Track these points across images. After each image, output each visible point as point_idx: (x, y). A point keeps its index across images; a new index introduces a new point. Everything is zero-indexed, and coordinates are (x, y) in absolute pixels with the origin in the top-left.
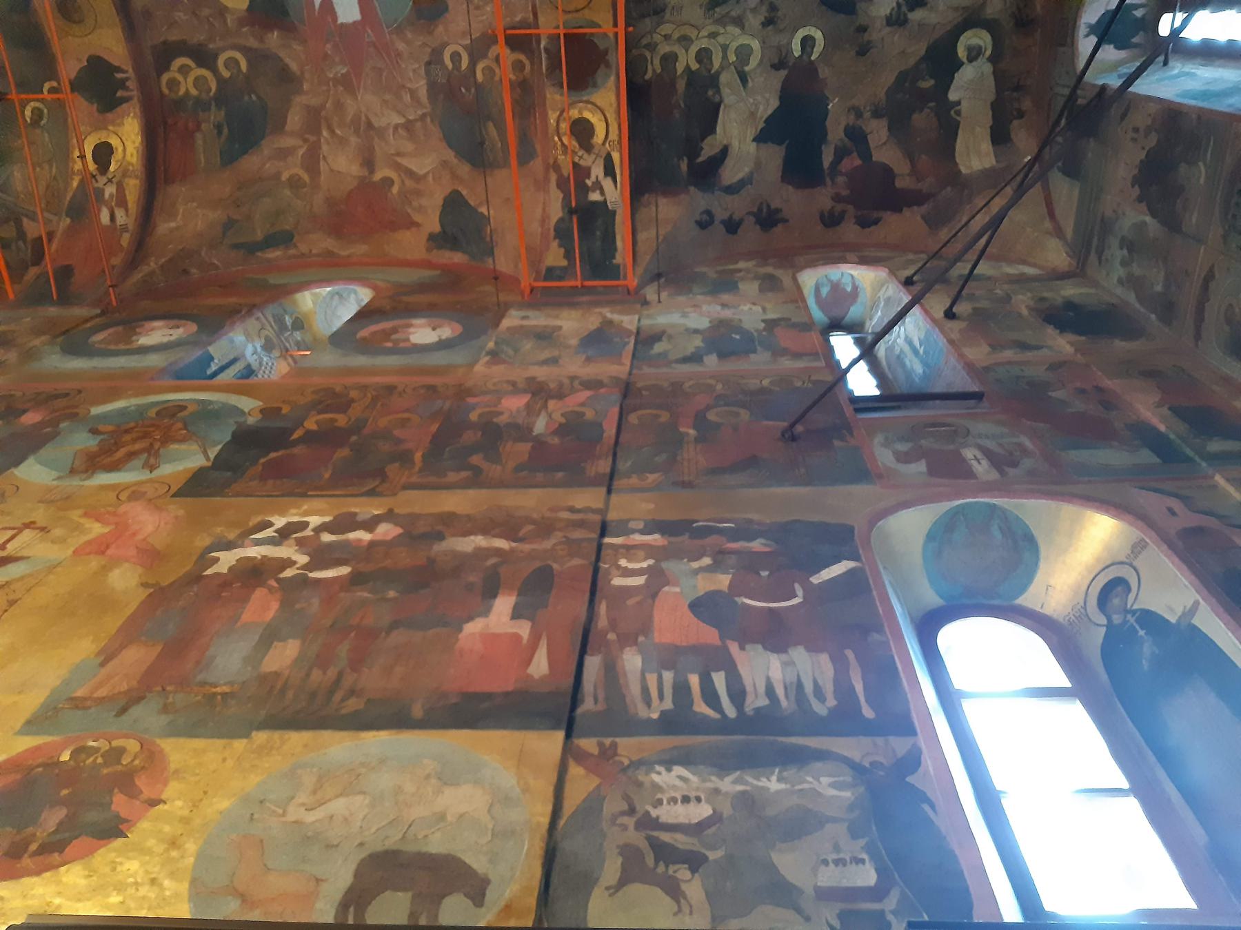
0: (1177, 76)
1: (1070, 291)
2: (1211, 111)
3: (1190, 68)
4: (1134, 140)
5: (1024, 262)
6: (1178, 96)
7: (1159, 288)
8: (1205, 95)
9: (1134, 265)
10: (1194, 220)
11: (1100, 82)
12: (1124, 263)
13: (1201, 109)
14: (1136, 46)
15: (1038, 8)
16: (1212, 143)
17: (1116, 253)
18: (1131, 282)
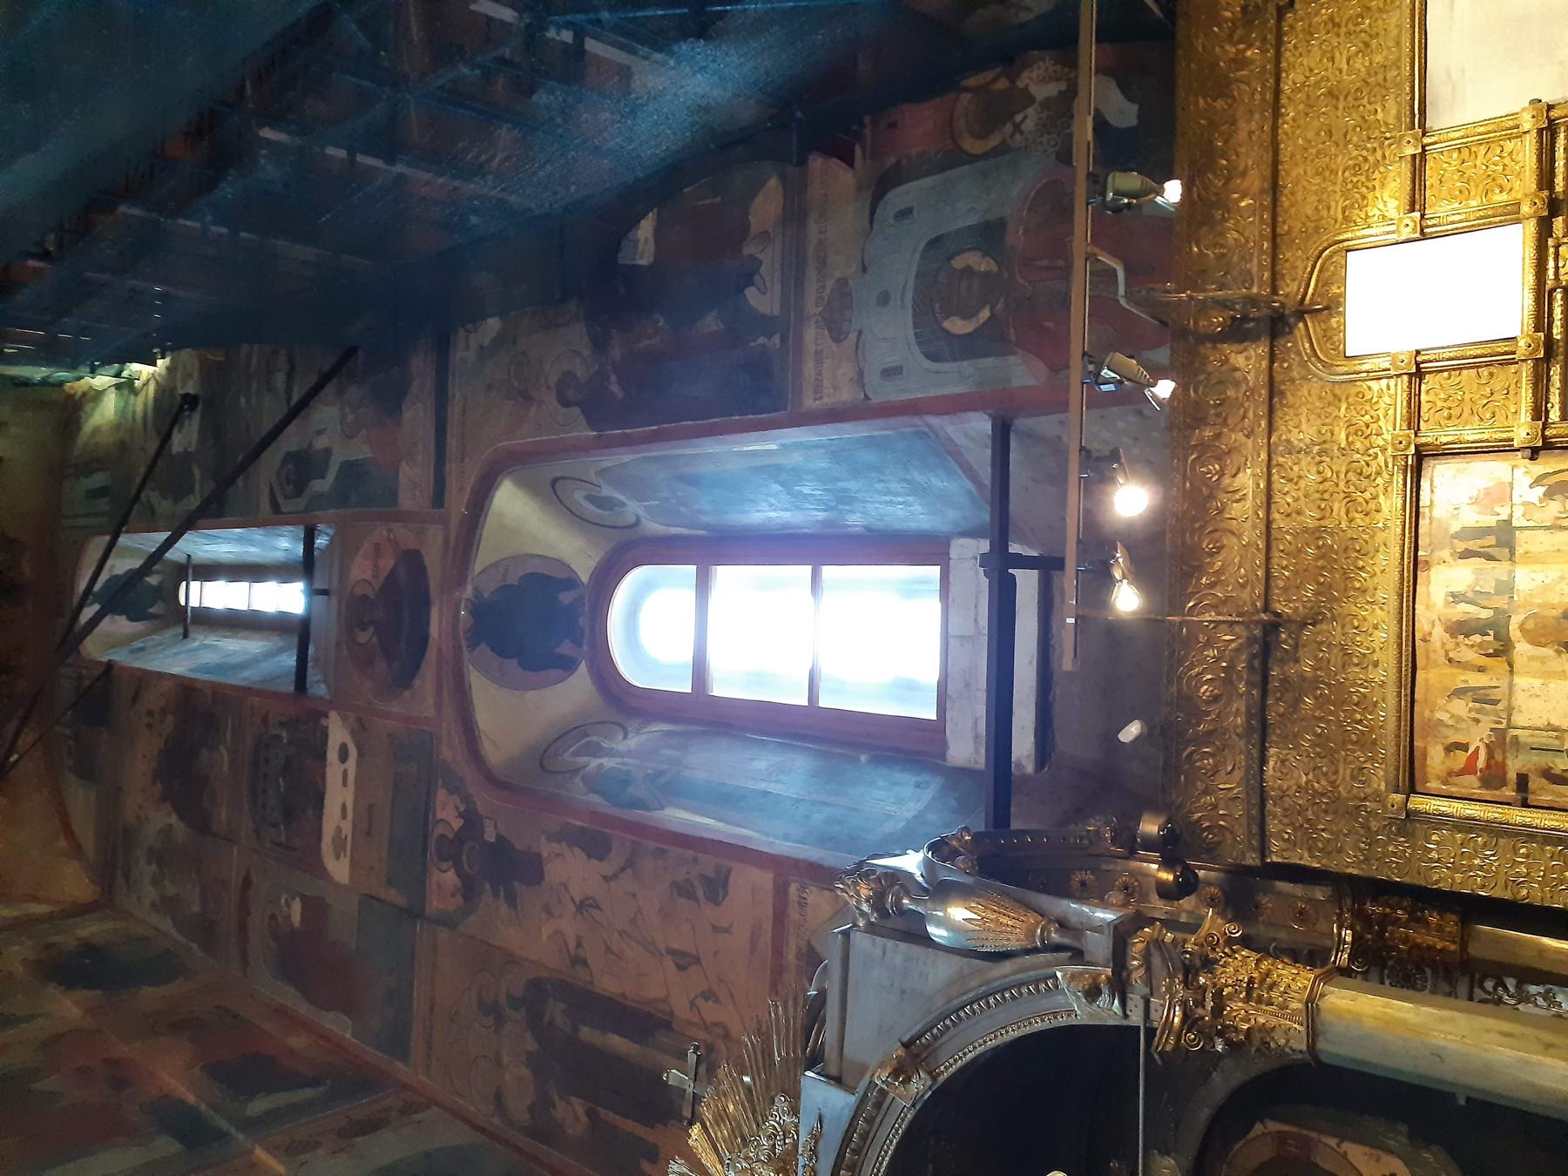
0: (197, 649)
1: (90, 929)
2: (226, 686)
3: (211, 640)
4: (149, 726)
5: (35, 899)
6: (192, 670)
7: (196, 908)
8: (221, 668)
9: (166, 882)
10: (223, 815)
11: (105, 659)
12: (156, 882)
13: (213, 683)
14: (154, 617)
15: (27, 571)
16: (230, 724)
17: (145, 870)
18: (168, 905)
